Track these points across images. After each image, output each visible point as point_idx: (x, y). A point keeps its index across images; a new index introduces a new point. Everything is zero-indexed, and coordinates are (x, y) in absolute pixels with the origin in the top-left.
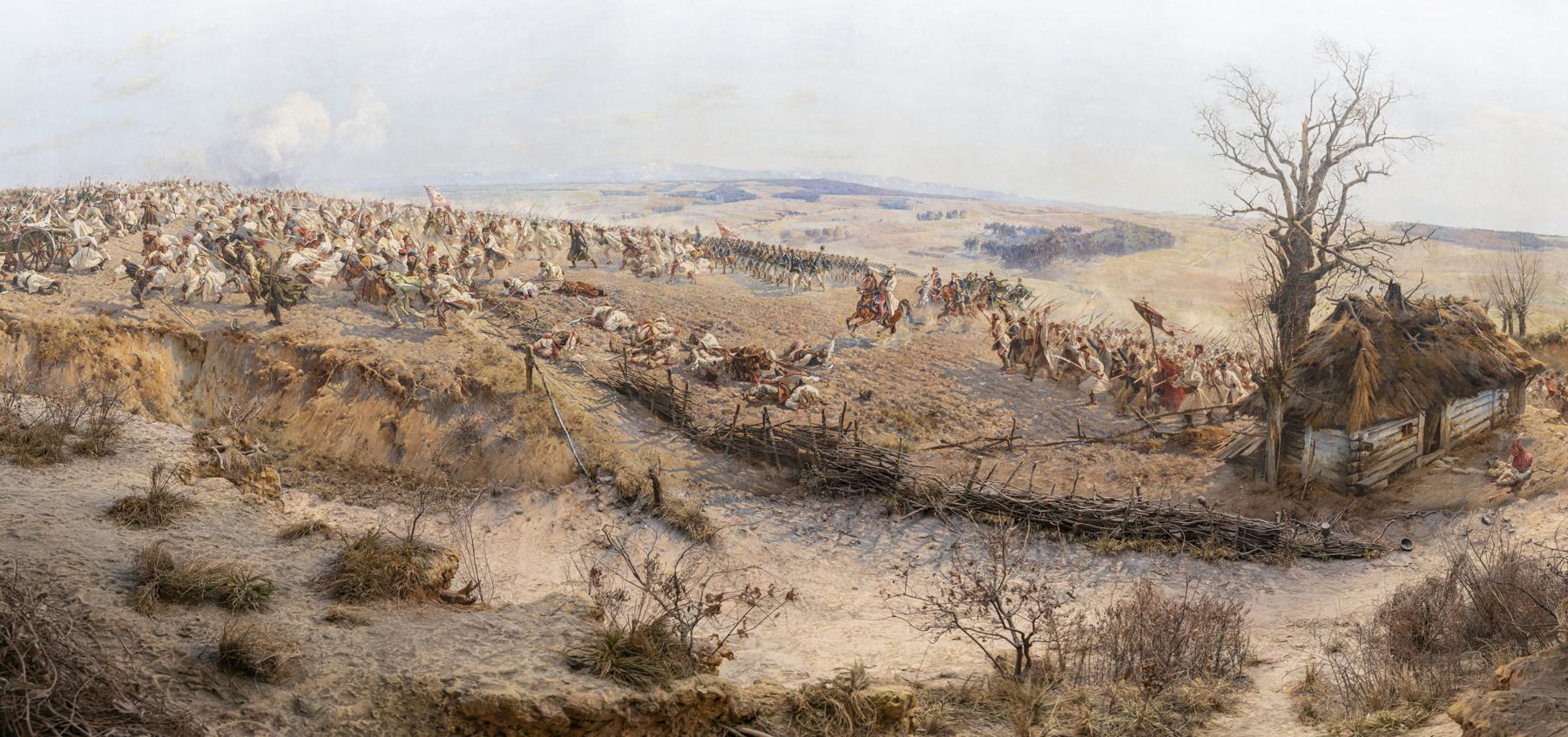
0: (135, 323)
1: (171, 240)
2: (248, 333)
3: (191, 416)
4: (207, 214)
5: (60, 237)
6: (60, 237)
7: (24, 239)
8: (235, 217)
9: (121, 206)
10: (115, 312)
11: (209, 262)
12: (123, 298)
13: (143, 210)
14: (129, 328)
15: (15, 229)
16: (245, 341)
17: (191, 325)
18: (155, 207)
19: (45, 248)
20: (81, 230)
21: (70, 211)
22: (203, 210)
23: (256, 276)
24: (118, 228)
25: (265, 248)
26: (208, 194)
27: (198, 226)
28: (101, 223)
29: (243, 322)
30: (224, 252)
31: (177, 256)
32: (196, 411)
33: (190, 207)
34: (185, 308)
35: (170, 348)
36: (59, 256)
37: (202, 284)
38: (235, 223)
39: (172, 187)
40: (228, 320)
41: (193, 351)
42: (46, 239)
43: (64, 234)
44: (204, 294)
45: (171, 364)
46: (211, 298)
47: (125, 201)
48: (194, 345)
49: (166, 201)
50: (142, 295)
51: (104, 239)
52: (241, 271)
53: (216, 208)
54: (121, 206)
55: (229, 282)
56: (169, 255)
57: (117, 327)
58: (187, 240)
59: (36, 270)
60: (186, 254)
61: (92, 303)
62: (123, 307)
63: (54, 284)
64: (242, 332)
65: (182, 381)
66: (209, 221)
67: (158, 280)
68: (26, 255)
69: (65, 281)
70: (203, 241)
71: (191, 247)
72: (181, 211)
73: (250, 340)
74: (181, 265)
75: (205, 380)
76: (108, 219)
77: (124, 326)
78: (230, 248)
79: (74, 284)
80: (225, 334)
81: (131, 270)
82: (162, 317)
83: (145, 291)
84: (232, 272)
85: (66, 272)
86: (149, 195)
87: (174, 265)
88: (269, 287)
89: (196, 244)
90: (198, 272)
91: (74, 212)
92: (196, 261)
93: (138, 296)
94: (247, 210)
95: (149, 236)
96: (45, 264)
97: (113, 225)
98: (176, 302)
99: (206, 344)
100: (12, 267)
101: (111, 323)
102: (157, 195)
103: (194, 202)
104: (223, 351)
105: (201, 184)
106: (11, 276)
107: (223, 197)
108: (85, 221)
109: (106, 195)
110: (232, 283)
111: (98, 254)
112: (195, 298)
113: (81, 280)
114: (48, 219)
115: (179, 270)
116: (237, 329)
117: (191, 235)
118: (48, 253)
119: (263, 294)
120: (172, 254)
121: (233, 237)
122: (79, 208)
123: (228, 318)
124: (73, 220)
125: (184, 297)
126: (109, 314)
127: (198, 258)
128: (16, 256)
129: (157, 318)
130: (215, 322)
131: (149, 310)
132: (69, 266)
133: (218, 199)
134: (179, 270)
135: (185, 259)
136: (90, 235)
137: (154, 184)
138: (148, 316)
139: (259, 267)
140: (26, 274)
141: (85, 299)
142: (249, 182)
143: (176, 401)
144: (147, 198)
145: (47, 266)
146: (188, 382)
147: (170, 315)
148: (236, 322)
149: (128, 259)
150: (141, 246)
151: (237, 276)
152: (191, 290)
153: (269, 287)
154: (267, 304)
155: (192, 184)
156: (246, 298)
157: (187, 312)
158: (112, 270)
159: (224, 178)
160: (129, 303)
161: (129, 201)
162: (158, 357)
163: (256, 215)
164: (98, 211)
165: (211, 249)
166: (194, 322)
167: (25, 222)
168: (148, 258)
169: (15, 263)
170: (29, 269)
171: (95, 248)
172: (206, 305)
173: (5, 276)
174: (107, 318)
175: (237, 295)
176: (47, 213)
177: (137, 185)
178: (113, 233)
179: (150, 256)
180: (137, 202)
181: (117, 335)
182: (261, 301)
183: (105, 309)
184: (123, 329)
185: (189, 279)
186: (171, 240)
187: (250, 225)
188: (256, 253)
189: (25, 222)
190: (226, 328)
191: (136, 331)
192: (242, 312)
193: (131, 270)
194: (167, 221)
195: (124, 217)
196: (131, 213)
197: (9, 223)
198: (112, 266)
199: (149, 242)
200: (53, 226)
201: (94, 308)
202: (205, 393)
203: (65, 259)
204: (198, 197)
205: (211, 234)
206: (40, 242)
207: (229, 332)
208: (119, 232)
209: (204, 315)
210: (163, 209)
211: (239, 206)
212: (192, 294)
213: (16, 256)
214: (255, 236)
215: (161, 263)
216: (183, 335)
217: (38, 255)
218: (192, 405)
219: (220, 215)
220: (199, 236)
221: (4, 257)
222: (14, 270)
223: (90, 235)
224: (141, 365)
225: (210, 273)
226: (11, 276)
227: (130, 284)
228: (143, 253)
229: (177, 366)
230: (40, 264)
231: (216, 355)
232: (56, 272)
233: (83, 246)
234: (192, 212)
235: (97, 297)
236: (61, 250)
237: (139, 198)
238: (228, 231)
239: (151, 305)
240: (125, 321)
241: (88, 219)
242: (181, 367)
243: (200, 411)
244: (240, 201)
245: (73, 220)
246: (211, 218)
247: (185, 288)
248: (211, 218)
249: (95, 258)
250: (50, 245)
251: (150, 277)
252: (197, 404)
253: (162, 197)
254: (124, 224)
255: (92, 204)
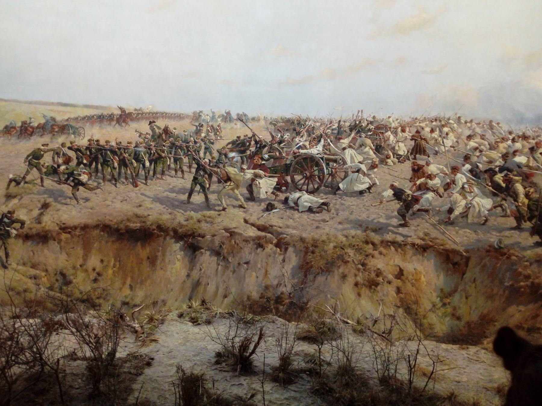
0: (400, 239)
1: (439, 169)
2: (512, 251)
3: (448, 319)
4: (476, 149)
5: (331, 164)
6: (331, 164)
7: (297, 163)
8: (504, 151)
9: (392, 137)
10: (380, 229)
11: (476, 189)
12: (388, 217)
13: (413, 143)
14: (393, 243)
15: (288, 154)
16: (509, 258)
17: (455, 242)
18: (425, 139)
19: (316, 173)
20: (352, 158)
21: (342, 141)
22: (472, 144)
23: (523, 203)
24: (388, 157)
25: (535, 179)
26: (479, 130)
27: (467, 158)
28: (371, 153)
29: (507, 242)
30: (492, 181)
31: (444, 183)
32: (453, 315)
33: (460, 141)
34: (450, 227)
35: (432, 261)
36: (330, 179)
37: (468, 208)
38: (505, 156)
39: (443, 123)
40: (492, 240)
41: (455, 264)
42: (318, 164)
43: (335, 161)
44: (470, 216)
45: (432, 274)
46: (476, 220)
47: (395, 133)
48: (457, 259)
49: (436, 135)
50: (408, 216)
51: (373, 166)
52: (509, 198)
53: (486, 143)
54: (392, 137)
55: (495, 207)
56: (436, 182)
57: (382, 242)
58: (455, 170)
59: (307, 192)
60: (454, 182)
61: (359, 221)
62: (389, 225)
63: (323, 204)
64: (506, 250)
65: (442, 290)
66: (478, 154)
67: (424, 203)
68: (297, 177)
69: (334, 201)
70: (471, 171)
71: (459, 175)
72: (451, 144)
73: (514, 258)
74: (448, 191)
75: (464, 290)
76: (378, 149)
77: (388, 242)
78: (499, 178)
79: (342, 204)
80: (488, 251)
81: (398, 194)
82: (426, 234)
83: (410, 212)
84: (499, 199)
85: (335, 194)
86: (419, 129)
87: (441, 190)
88: (536, 213)
89: (464, 174)
90: (465, 198)
91: (345, 142)
92: (463, 188)
93: (403, 217)
94: (518, 145)
95: (418, 165)
96: (316, 187)
97: (382, 154)
98: (440, 222)
99: (468, 259)
100: (284, 188)
101: (376, 238)
102: (428, 129)
103: (464, 137)
104: (484, 266)
105: (471, 121)
106: (282, 196)
107: (494, 133)
108: (356, 150)
109: (377, 128)
110: (499, 209)
111: (367, 180)
112: (460, 220)
113: (350, 201)
114: (320, 147)
115: (446, 195)
116: (500, 248)
117: (459, 166)
118: (319, 177)
119: (530, 219)
120: (439, 182)
121: (502, 169)
122: (350, 138)
123: (493, 239)
124: (344, 149)
125: (449, 218)
126: (375, 231)
127: (466, 186)
128: (288, 179)
129: (421, 235)
130: (478, 241)
131: (413, 228)
132: (339, 188)
133: (489, 134)
134: (446, 195)
135: (453, 186)
136: (360, 162)
137: (425, 120)
138: (412, 234)
139: (527, 195)
140: (297, 195)
141: (352, 217)
142: (521, 120)
143: (434, 306)
144: (418, 132)
145: (318, 188)
146: (447, 290)
147: (434, 233)
148: (500, 241)
149: (396, 184)
150: (409, 174)
151: (504, 202)
152: (457, 212)
153: (536, 213)
154: (533, 228)
155: (463, 121)
156: (512, 222)
157: (451, 231)
158: (379, 193)
159: (496, 115)
160: (395, 222)
161: (400, 134)
162: (420, 268)
163: (526, 150)
164: (369, 141)
165: (479, 178)
166: (458, 240)
167: (298, 148)
168: (415, 184)
169: (286, 184)
170: (300, 190)
171: (364, 174)
172: (468, 226)
173: (277, 196)
174: (373, 234)
175: (503, 219)
176: (320, 141)
177: (408, 119)
178: (383, 161)
179: (418, 182)
180: (408, 134)
181: (382, 249)
182: (528, 225)
183: (370, 227)
184: (387, 244)
185: (455, 203)
186: (439, 169)
187: (521, 159)
188: (525, 184)
189: (298, 148)
190: (490, 246)
191: (400, 246)
192: (507, 233)
193: (398, 194)
194: (436, 153)
195: (393, 149)
196: (401, 145)
197: (282, 148)
198: (380, 190)
199: (418, 171)
200: (325, 154)
201: (361, 226)
202: (464, 299)
203: (335, 182)
204: (468, 133)
205: (480, 166)
206: (312, 167)
207: (491, 249)
208: (389, 161)
209: (468, 235)
210: (433, 142)
211: (510, 142)
212: (457, 217)
213: (288, 179)
214: (525, 169)
215: (428, 189)
216: (447, 251)
217: (310, 178)
218: (449, 310)
219: (490, 149)
220: (468, 166)
221: (276, 179)
222: (286, 191)
223: (360, 162)
224: (403, 275)
225: (477, 199)
226: (282, 196)
227: (397, 205)
228: (411, 180)
229: (438, 276)
230: (311, 186)
231: (478, 269)
232: (326, 194)
233: (353, 172)
234: (461, 146)
235: (363, 216)
236: (331, 175)
237: (410, 132)
238: (497, 163)
239: (416, 224)
240: (389, 237)
241: (358, 148)
242: (442, 277)
243: (457, 314)
244: (511, 137)
245: (344, 149)
246: (481, 151)
247: (451, 211)
248: (481, 151)
249: (363, 183)
250: (321, 170)
251: (416, 200)
252: (455, 309)
253: (432, 131)
254: (394, 154)
255: (363, 135)
